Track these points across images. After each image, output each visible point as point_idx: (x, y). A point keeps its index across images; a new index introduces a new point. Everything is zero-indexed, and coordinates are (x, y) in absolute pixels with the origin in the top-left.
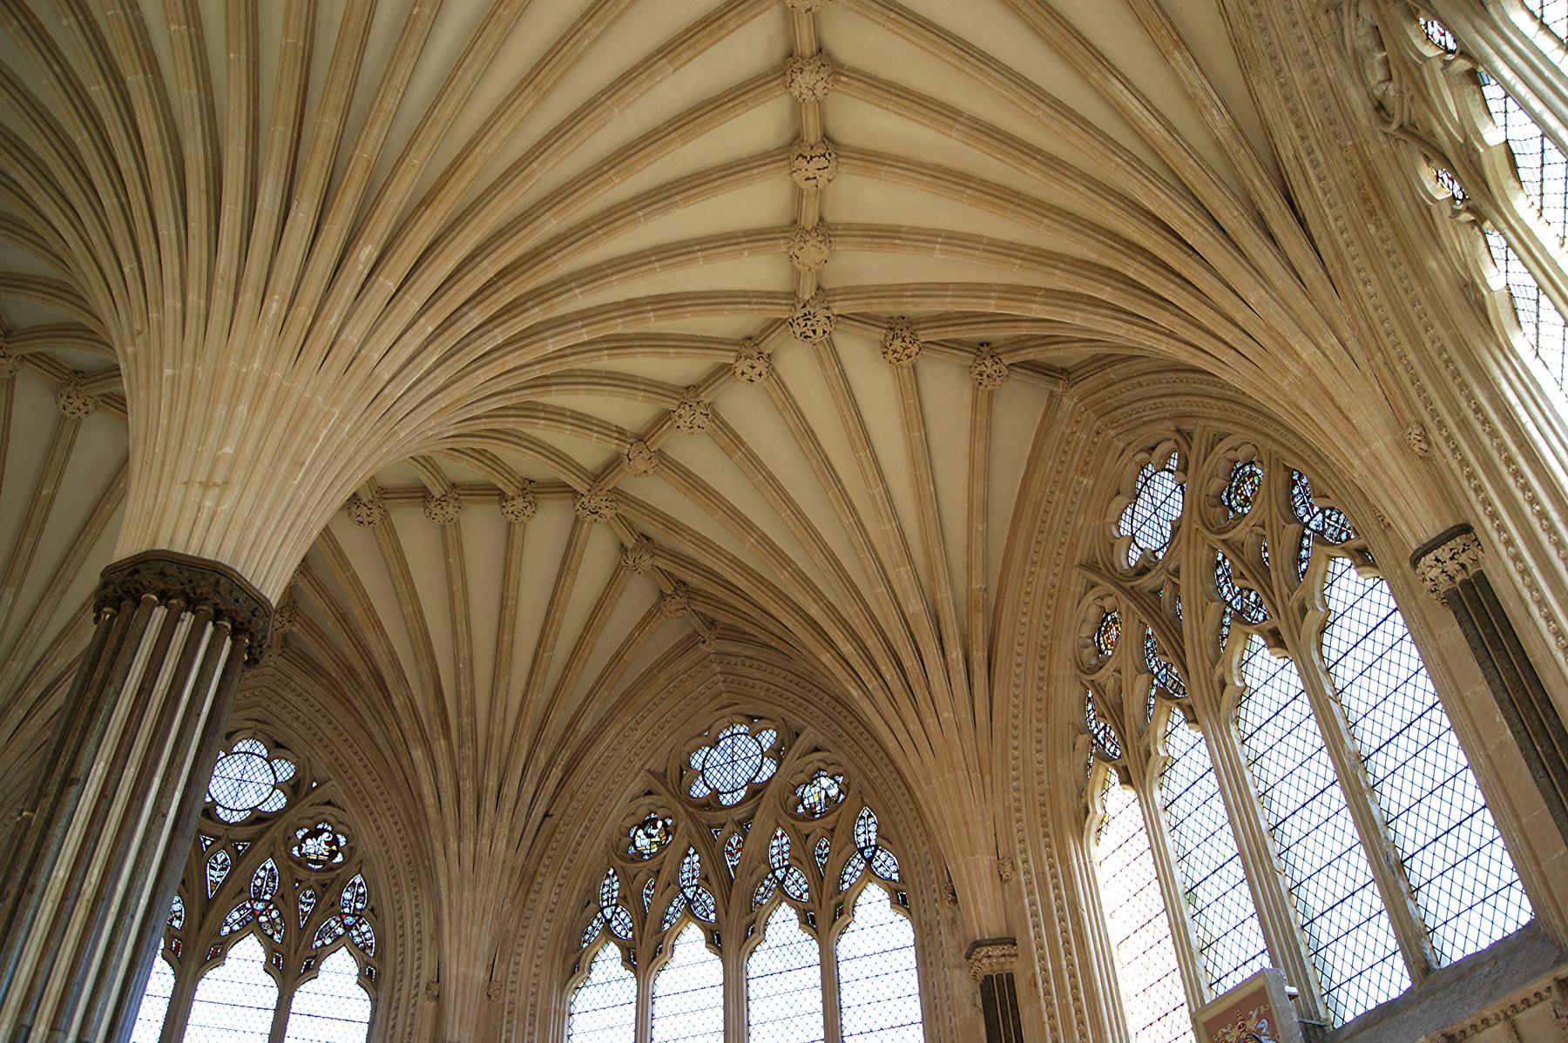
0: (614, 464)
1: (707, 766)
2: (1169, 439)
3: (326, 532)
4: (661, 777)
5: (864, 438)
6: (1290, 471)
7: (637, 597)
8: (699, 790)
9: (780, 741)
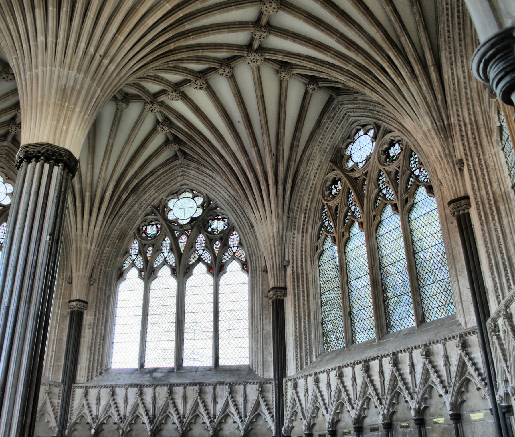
0: (163, 92)
1: (174, 208)
2: (371, 125)
3: (13, 78)
4: (156, 208)
5: (262, 98)
6: (412, 151)
7: (158, 140)
8: (171, 216)
9: (204, 202)
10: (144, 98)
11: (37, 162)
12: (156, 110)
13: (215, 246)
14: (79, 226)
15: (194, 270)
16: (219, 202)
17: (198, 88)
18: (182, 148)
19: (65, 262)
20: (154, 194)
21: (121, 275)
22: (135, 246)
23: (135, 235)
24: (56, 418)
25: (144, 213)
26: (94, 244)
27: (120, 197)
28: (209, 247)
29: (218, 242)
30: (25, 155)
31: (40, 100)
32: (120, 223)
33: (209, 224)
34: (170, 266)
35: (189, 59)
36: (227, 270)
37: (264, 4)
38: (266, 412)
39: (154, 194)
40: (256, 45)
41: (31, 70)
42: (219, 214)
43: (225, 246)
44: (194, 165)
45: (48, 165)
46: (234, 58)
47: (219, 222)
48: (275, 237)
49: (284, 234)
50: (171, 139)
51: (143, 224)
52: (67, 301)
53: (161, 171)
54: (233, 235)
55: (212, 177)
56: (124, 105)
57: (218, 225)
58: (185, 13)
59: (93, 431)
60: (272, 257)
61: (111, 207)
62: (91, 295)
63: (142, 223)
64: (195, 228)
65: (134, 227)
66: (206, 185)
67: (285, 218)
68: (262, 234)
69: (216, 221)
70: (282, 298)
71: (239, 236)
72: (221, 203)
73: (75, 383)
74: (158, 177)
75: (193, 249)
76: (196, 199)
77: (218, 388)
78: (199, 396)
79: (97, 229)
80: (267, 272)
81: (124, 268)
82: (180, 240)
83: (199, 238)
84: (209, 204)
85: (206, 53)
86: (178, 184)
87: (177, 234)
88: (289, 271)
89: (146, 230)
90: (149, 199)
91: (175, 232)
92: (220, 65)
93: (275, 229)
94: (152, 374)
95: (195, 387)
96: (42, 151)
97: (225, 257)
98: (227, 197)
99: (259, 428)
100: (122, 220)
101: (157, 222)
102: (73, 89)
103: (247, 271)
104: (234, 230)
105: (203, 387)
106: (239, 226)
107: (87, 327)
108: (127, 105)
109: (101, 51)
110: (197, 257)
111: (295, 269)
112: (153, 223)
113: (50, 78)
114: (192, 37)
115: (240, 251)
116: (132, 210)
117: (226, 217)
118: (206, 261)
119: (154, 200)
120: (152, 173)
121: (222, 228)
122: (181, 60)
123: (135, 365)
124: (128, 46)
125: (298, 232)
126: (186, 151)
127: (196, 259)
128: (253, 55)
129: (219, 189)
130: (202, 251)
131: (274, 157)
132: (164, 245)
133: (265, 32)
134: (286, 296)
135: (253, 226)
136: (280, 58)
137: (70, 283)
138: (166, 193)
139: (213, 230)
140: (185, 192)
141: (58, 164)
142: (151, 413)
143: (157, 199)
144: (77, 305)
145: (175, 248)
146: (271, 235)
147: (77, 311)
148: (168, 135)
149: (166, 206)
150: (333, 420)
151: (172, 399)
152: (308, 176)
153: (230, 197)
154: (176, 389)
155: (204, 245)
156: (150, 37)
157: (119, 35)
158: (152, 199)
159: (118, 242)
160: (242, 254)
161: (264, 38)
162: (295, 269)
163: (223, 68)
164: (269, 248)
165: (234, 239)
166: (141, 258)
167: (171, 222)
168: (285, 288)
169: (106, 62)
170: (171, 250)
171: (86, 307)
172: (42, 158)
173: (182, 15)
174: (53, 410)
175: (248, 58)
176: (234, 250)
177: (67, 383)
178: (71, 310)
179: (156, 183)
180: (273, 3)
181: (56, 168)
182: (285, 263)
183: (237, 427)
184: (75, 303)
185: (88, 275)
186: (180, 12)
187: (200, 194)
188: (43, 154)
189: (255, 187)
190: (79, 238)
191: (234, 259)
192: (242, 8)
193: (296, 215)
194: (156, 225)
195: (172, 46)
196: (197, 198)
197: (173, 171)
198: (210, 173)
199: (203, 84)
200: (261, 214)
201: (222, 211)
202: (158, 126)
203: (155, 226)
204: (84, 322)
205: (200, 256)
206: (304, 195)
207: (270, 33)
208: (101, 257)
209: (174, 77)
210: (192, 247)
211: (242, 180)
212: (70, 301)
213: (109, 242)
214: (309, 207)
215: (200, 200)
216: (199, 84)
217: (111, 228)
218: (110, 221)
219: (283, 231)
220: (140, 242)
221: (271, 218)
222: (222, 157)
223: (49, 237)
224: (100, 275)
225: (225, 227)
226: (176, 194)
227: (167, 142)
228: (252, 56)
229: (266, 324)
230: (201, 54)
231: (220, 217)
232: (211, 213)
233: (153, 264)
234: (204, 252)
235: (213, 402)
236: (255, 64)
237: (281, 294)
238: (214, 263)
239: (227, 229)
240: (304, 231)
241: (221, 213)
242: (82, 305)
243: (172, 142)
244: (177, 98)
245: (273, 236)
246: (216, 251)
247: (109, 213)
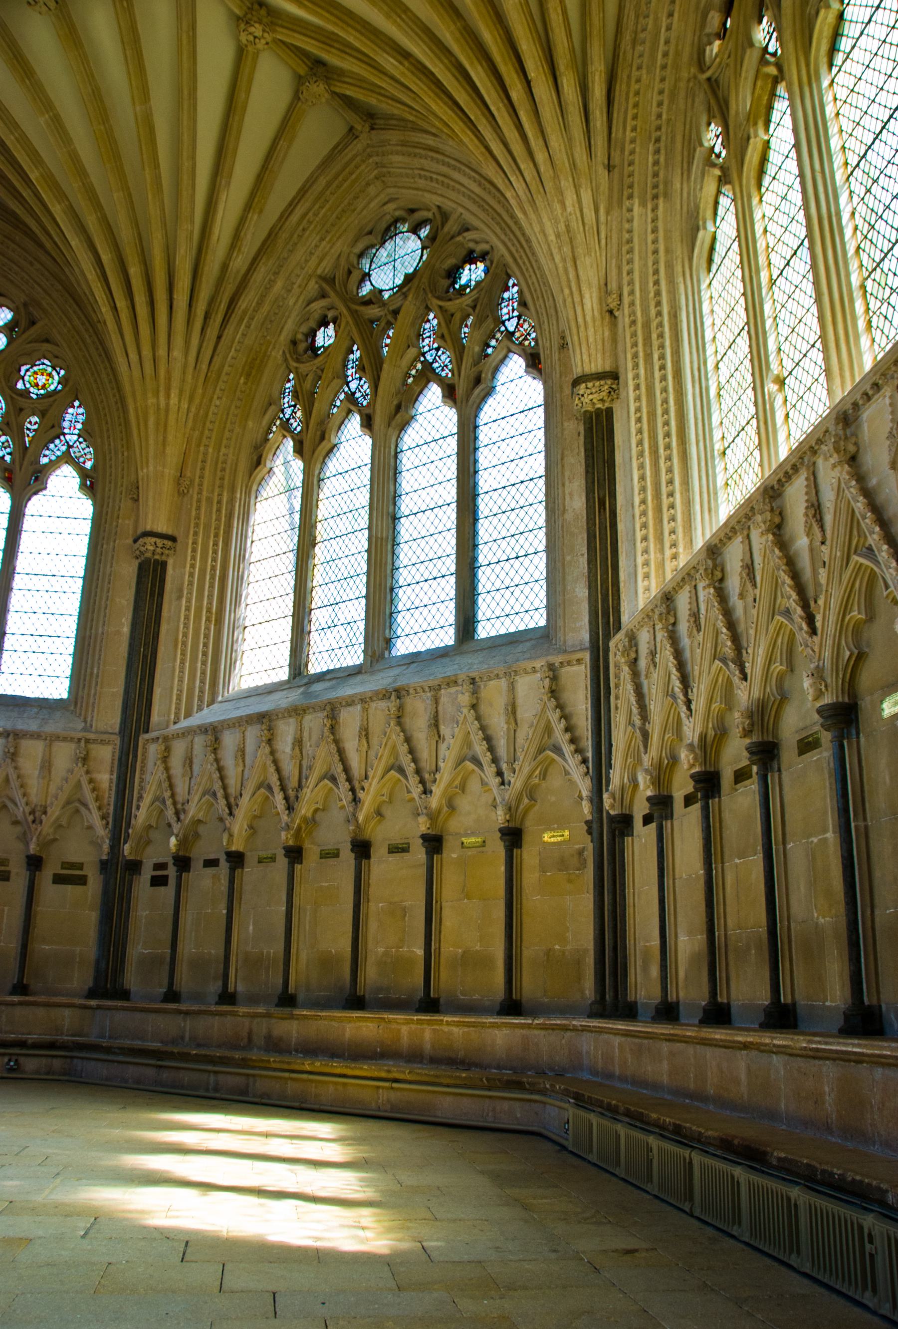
4: (330, 280)
14: (134, 357)
18: (338, 90)
19: (126, 454)
20: (317, 246)
23: (286, 360)
24: (103, 817)
38: (568, 749)
39: (317, 246)
47: (473, 266)
53: (322, 181)
55: (436, 151)
57: (472, 274)
59: (173, 841)
64: (410, 298)
65: (282, 338)
69: (467, 267)
74: (317, 199)
75: (412, 352)
77: (445, 695)
83: (428, 321)
90: (307, 261)
98: (477, 190)
99: (553, 799)
104: (509, 277)
116: (271, 297)
119: (321, 260)
125: (643, 204)
126: (348, 93)
130: (434, 352)
142: (293, 783)
143: (328, 258)
150: (703, 738)
152: (651, 21)
153: (480, 185)
159: (245, 383)
174: (97, 799)
178: (139, 561)
179: (316, 215)
183: (490, 801)
191: (510, 351)
193: (632, 152)
197: (351, 174)
204: (168, 586)
208: (204, 424)
213: (221, 385)
218: (212, 332)
222: (405, 55)
224: (203, 469)
229: (571, 494)
234: (440, 353)
242: (160, 545)
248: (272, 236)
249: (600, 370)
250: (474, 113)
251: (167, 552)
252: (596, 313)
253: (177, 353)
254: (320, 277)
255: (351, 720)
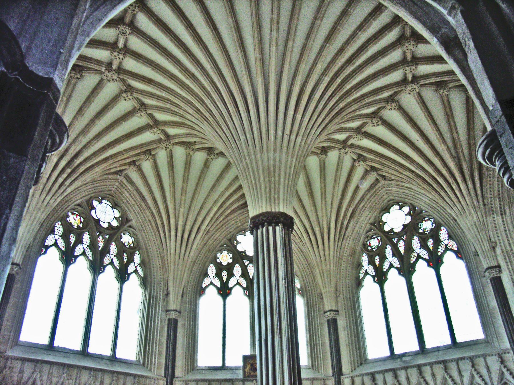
4: (373, 224)
8: (387, 228)
9: (410, 210)
10: (336, 146)
11: (263, 228)
12: (349, 152)
13: (428, 243)
14: (317, 254)
15: (416, 266)
16: (422, 207)
17: (376, 125)
21: (359, 284)
22: (365, 259)
23: (362, 250)
25: (365, 231)
26: (332, 265)
27: (342, 224)
28: (424, 245)
29: (430, 240)
30: (254, 224)
31: (253, 182)
32: (348, 244)
33: (419, 226)
34: (397, 268)
35: (359, 109)
36: (444, 261)
37: (404, 45)
40: (410, 77)
41: (242, 162)
42: (425, 216)
43: (437, 242)
44: (393, 183)
45: (272, 227)
46: (396, 94)
48: (477, 225)
49: (485, 220)
50: (369, 169)
51: (366, 240)
52: (322, 312)
53: (369, 195)
54: (441, 230)
55: (411, 189)
56: (324, 156)
57: (427, 226)
58: (342, 78)
60: (479, 242)
61: (338, 234)
62: (339, 304)
63: (365, 238)
66: (408, 196)
67: (482, 206)
68: (465, 225)
69: (424, 222)
70: (498, 275)
71: (447, 230)
72: (425, 207)
73: (342, 375)
75: (412, 250)
76: (403, 209)
78: (446, 372)
79: (332, 253)
80: (478, 255)
81: (361, 277)
82: (399, 245)
84: (415, 210)
85: (371, 99)
86: (385, 201)
87: (395, 240)
88: (498, 251)
89: (370, 244)
91: (393, 239)
92: (386, 102)
93: (475, 218)
94: (402, 359)
95: (440, 365)
96: (265, 219)
97: (439, 250)
98: (427, 201)
100: (349, 241)
101: (377, 235)
102: (274, 167)
103: (461, 258)
104: (441, 226)
105: (446, 364)
106: (444, 222)
107: (342, 329)
108: (326, 155)
109: (287, 131)
110: (416, 255)
111: (503, 248)
112: (374, 237)
113: (256, 163)
114: (354, 92)
115: (451, 243)
117: (432, 217)
118: (424, 258)
119: (370, 218)
120: (362, 198)
121: (431, 228)
122: (354, 111)
123: (388, 353)
124: (306, 120)
126: (383, 174)
127: (415, 258)
128: (410, 86)
129: (419, 196)
131: (456, 159)
132: (387, 252)
133: (413, 65)
134: (502, 272)
135: (456, 220)
136: (433, 80)
137: (322, 298)
138: (378, 211)
139: (424, 230)
140: (393, 206)
141: (278, 224)
144: (330, 314)
145: (396, 253)
146: (473, 224)
147: (332, 319)
148: (365, 167)
149: (380, 221)
151: (423, 377)
153: (430, 200)
154: (424, 369)
155: (419, 245)
156: (321, 106)
157: (297, 114)
158: (368, 218)
160: (453, 245)
161: (414, 70)
162: (503, 248)
163: (389, 104)
164: (474, 236)
165: (443, 234)
166: (372, 267)
167: (388, 232)
168: (499, 267)
169: (293, 137)
170: (394, 255)
171: (338, 314)
172: (266, 224)
173: (340, 81)
175: (407, 89)
176: (446, 242)
177: (336, 377)
180: (411, 41)
181: (278, 229)
182: (493, 245)
184: (328, 313)
185: (333, 289)
186: (338, 79)
187: (405, 205)
188: (265, 221)
189: (447, 188)
190: (319, 264)
191: (447, 250)
192: (386, 55)
194: (377, 237)
195: (341, 105)
196: (404, 208)
198: (409, 186)
199: (378, 121)
200: (460, 209)
201: (426, 213)
202: (355, 163)
203: (376, 239)
205: (418, 254)
206: (493, 182)
207: (417, 64)
209: (355, 124)
210: (410, 249)
211: (435, 185)
212: (325, 313)
213: (344, 260)
214: (501, 191)
215: (406, 209)
216: (375, 123)
217: (342, 249)
218: (340, 244)
219: (483, 217)
220: (368, 255)
221: (469, 210)
222: (413, 172)
223: (284, 281)
225: (433, 225)
226: (387, 209)
227: (366, 172)
228: (409, 88)
230: (367, 101)
231: (426, 219)
232: (418, 217)
233: (382, 269)
235: (460, 376)
236: (415, 92)
237: (496, 272)
238: (431, 258)
239: (435, 227)
240: (503, 213)
241: (427, 215)
243: (371, 171)
244: (361, 138)
245: (475, 225)
246: (431, 246)
247: (337, 239)
248: (353, 212)
249: (494, 265)
250: (439, 190)
251: (337, 316)
252: (489, 248)
253: (332, 253)
254: (370, 224)
255: (427, 372)
